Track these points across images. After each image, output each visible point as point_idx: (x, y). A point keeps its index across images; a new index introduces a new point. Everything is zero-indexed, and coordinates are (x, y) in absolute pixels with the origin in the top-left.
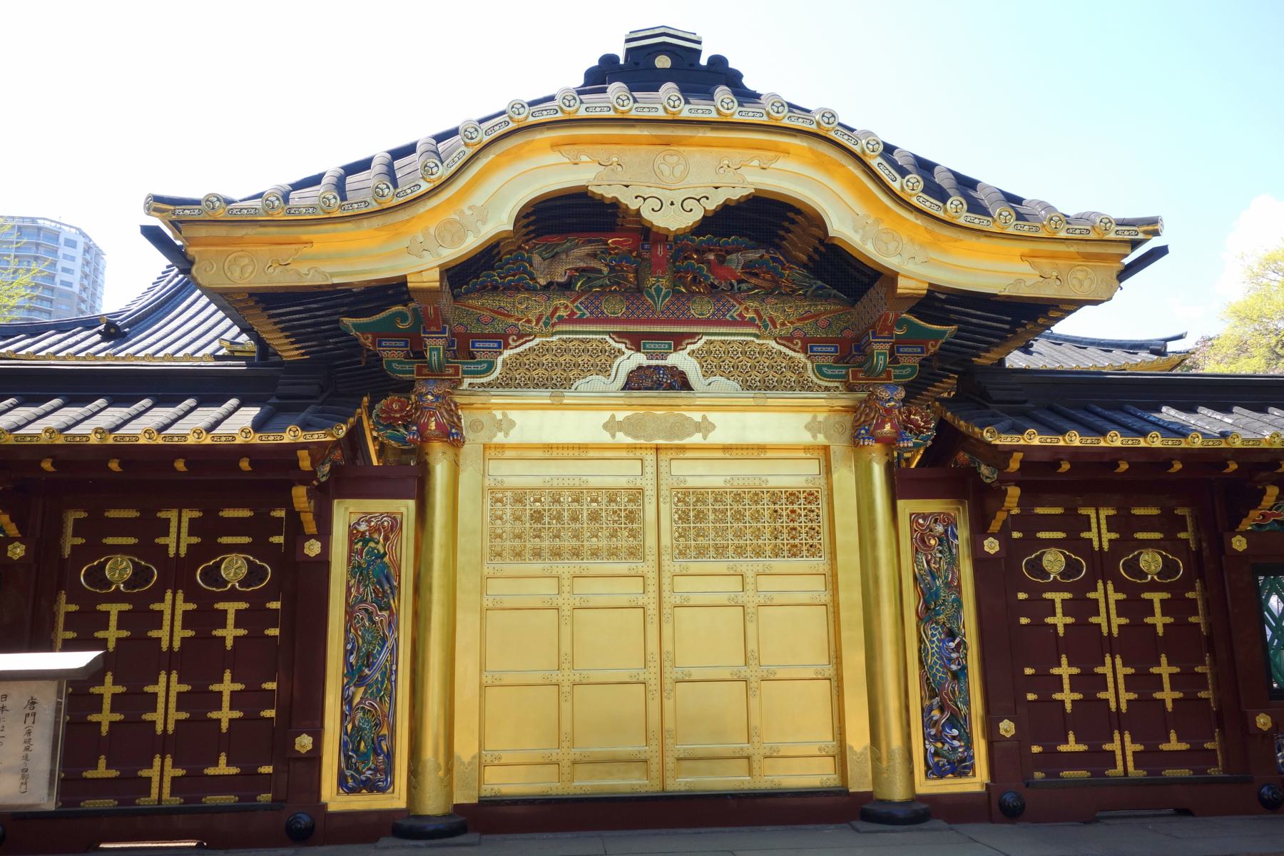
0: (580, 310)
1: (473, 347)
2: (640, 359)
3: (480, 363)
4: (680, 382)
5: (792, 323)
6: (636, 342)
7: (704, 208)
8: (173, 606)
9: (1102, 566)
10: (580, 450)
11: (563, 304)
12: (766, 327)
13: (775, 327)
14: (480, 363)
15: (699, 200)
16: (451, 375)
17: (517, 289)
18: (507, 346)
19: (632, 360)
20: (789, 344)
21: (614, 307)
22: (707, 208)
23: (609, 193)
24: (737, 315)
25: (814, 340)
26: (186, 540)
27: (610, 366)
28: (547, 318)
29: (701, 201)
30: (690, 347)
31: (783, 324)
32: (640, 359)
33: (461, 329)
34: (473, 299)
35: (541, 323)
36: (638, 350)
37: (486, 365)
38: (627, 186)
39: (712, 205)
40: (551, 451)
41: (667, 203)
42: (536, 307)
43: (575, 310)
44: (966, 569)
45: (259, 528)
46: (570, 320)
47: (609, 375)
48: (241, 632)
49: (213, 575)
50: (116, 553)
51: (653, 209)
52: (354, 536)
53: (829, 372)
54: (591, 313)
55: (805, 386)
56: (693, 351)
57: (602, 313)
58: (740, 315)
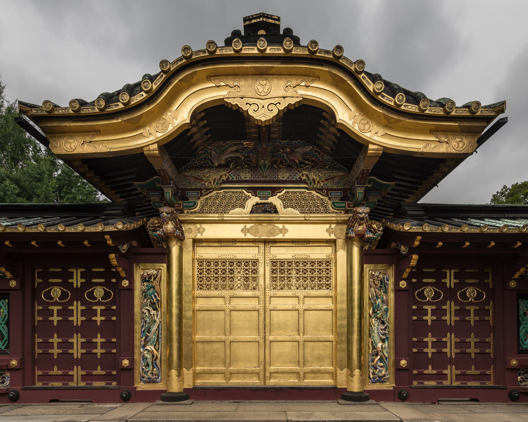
0: (231, 177)
1: (187, 195)
2: (257, 200)
3: (191, 202)
5: (322, 182)
6: (255, 191)
7: (278, 109)
8: (77, 307)
11: (224, 174)
12: (311, 183)
13: (315, 184)
14: (191, 202)
15: (276, 105)
16: (177, 207)
17: (205, 167)
18: (201, 195)
19: (254, 200)
20: (320, 192)
21: (246, 175)
22: (280, 109)
23: (233, 102)
24: (299, 178)
25: (332, 189)
26: (80, 281)
27: (245, 204)
28: (218, 181)
29: (277, 105)
30: (279, 194)
31: (318, 182)
32: (257, 200)
33: (182, 187)
34: (187, 172)
35: (215, 183)
36: (256, 196)
37: (193, 203)
38: (242, 98)
39: (281, 107)
41: (261, 107)
43: (230, 177)
47: (244, 208)
48: (103, 318)
49: (91, 295)
50: (55, 286)
51: (254, 110)
53: (338, 205)
54: (236, 178)
56: (280, 196)
57: (241, 178)
58: (300, 178)
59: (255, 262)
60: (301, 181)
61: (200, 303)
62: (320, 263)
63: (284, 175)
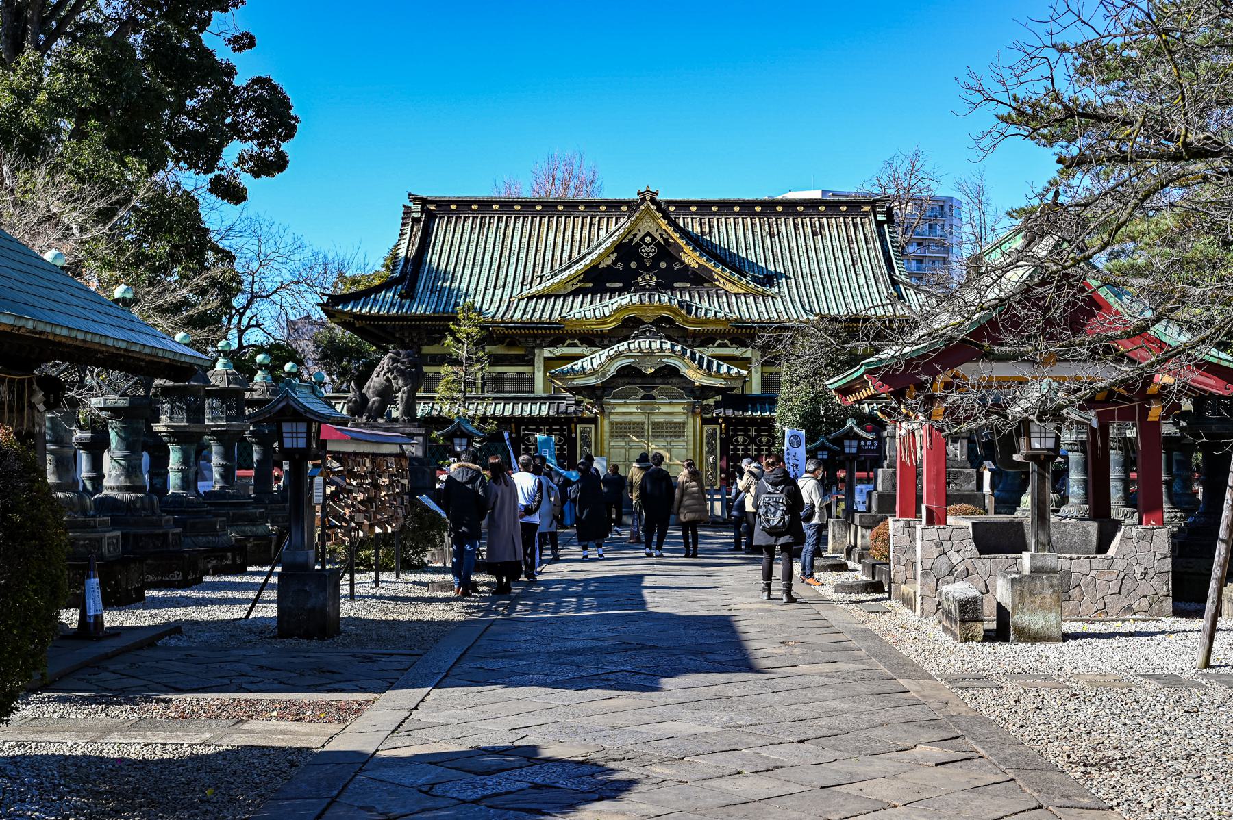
2: (645, 393)
4: (653, 398)
6: (643, 388)
9: (753, 440)
10: (631, 414)
11: (626, 380)
19: (643, 393)
21: (639, 381)
32: (645, 393)
40: (624, 414)
42: (620, 381)
44: (718, 441)
45: (562, 430)
46: (628, 384)
52: (581, 432)
55: (682, 398)
59: (643, 423)
60: (667, 384)
61: (612, 444)
62: (679, 423)
63: (658, 381)
